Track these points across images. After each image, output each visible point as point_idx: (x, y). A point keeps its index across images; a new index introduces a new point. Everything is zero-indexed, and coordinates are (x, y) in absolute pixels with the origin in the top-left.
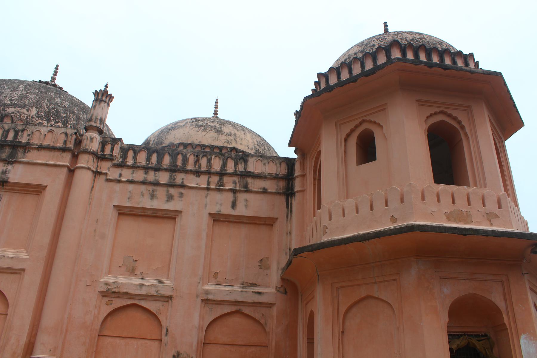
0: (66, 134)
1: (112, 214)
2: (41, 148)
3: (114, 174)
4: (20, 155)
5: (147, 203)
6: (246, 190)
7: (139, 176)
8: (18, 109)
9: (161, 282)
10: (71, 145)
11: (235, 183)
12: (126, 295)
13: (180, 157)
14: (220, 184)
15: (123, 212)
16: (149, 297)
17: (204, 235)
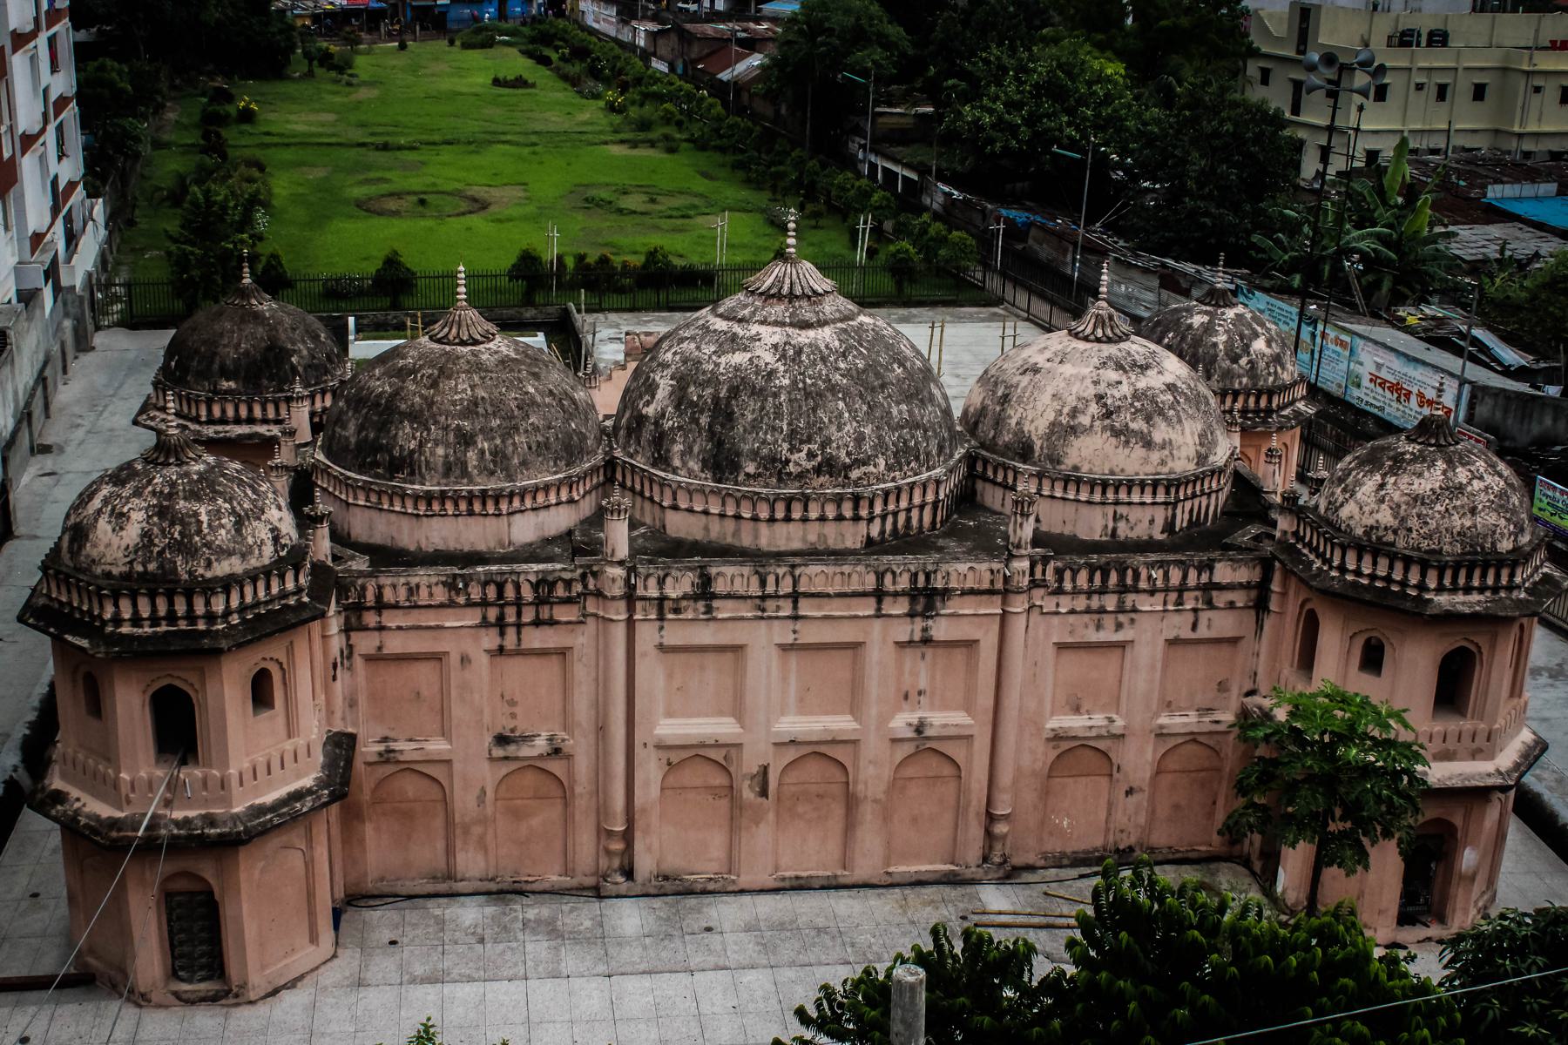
0: (992, 571)
1: (1051, 652)
2: (964, 593)
3: (1049, 604)
4: (938, 604)
5: (1093, 636)
6: (1210, 604)
7: (1081, 603)
8: (863, 469)
9: (1111, 720)
10: (999, 585)
11: (1197, 599)
12: (1075, 738)
13: (1130, 572)
14: (1179, 602)
15: (1061, 647)
16: (1099, 737)
17: (1159, 665)
